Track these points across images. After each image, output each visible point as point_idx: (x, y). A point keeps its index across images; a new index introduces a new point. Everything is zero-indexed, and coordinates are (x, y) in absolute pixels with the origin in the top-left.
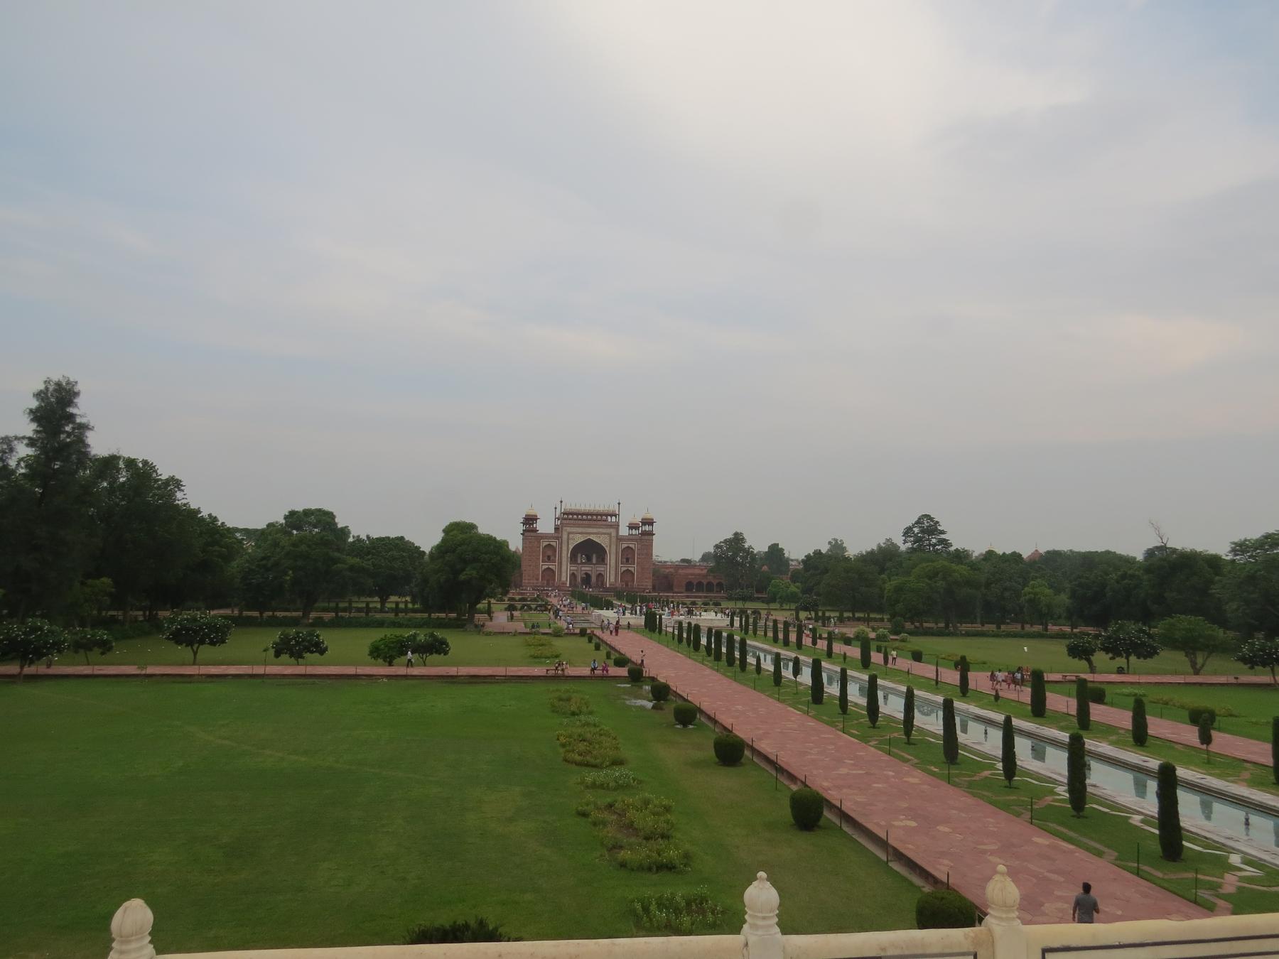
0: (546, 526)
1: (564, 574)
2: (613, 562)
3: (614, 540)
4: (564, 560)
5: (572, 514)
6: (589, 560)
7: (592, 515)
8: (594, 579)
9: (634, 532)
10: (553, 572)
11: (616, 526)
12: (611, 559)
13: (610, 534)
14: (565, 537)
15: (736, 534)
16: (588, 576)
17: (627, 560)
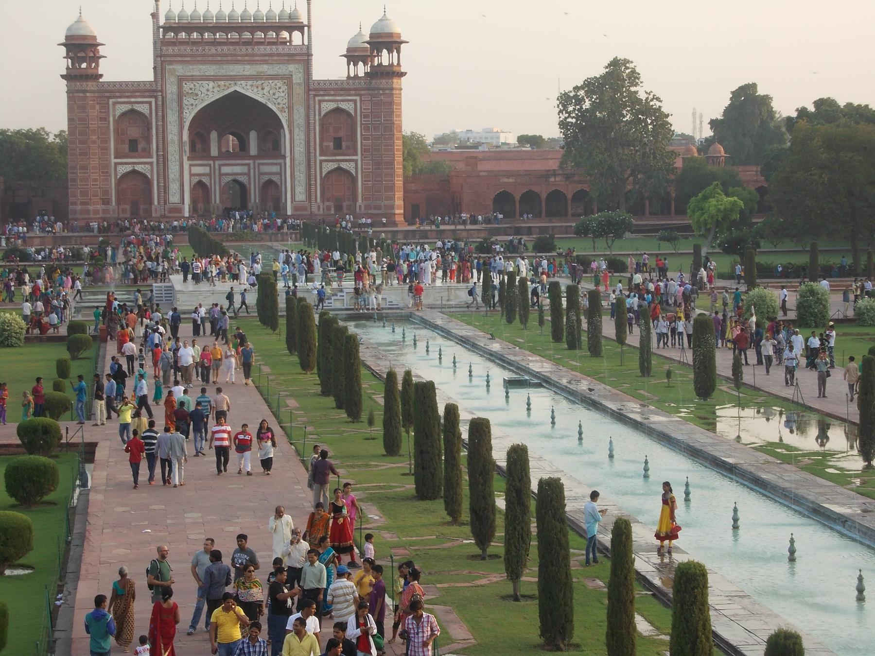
0: (128, 60)
1: (174, 187)
2: (300, 149)
3: (299, 91)
4: (173, 150)
5: (189, 28)
6: (243, 145)
7: (239, 28)
8: (254, 197)
9: (361, 70)
10: (146, 180)
11: (304, 57)
12: (294, 142)
13: (288, 79)
14: (171, 89)
15: (616, 64)
16: (243, 189)
17: (338, 143)
